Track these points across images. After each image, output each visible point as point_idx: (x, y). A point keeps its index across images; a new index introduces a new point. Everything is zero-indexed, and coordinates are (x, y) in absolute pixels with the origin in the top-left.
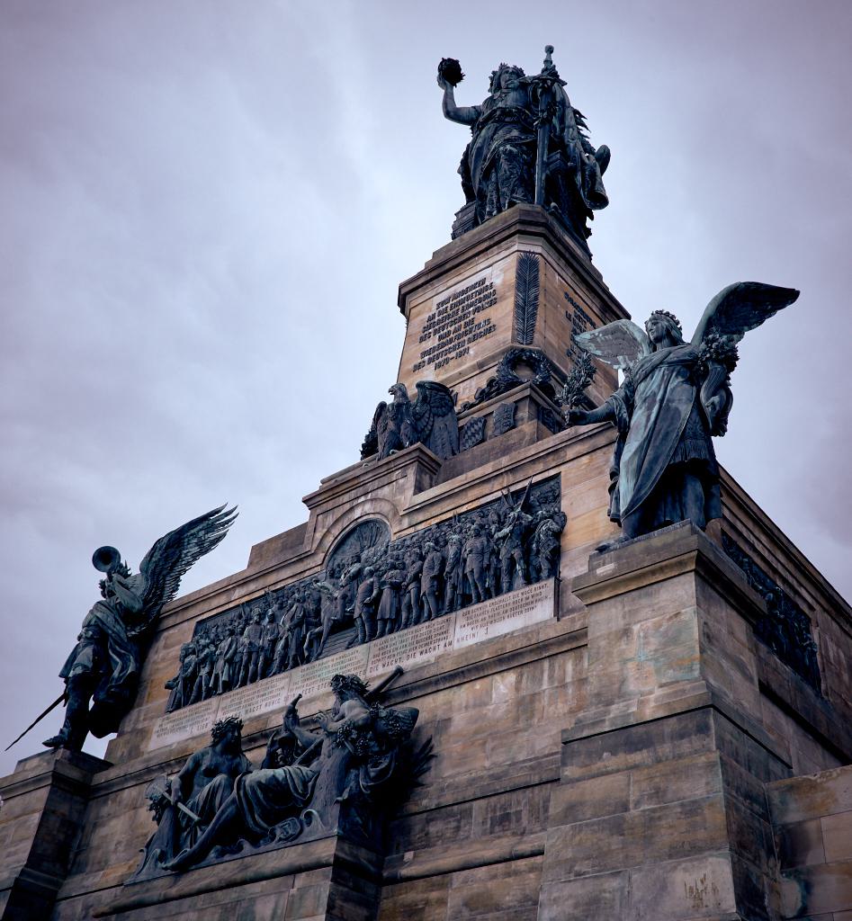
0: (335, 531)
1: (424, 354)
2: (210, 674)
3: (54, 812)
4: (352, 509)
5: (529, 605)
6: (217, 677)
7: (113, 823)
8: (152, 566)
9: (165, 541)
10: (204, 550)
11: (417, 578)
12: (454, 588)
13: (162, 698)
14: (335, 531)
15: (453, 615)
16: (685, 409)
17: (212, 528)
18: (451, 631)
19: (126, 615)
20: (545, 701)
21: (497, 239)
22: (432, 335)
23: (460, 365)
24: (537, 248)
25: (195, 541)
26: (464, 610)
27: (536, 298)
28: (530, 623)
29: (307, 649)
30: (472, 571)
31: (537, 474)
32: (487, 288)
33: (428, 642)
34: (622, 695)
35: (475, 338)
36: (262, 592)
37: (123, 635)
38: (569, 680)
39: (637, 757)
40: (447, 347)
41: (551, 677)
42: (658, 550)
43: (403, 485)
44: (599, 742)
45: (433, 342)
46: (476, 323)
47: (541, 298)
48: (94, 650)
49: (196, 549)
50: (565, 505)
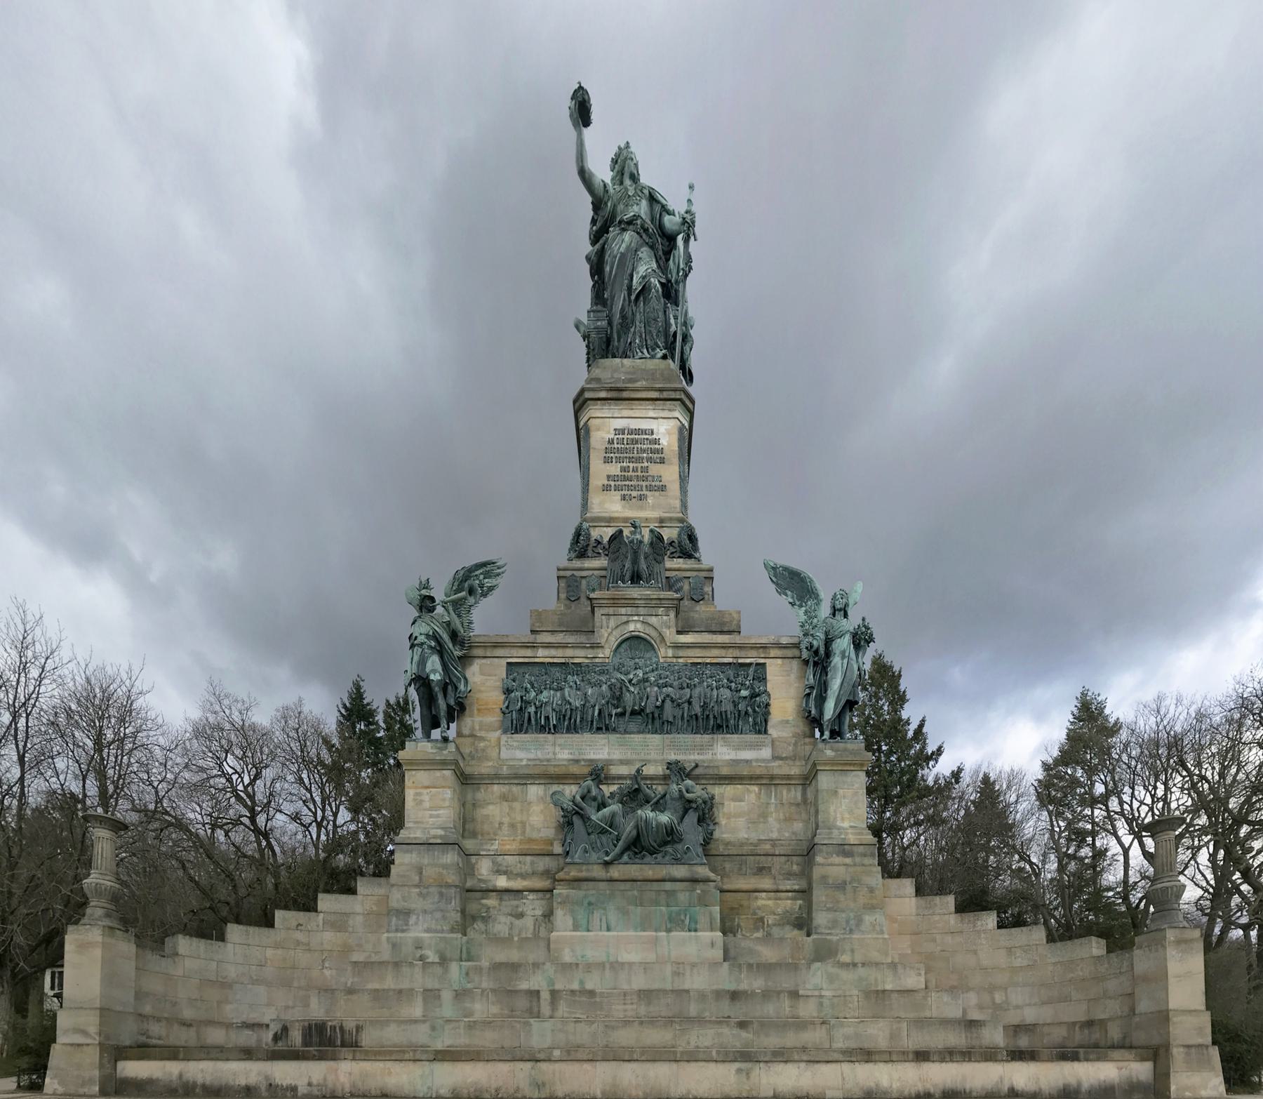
2: (536, 713)
6: (547, 718)
13: (494, 718)
39: (848, 861)
44: (831, 849)
50: (769, 688)
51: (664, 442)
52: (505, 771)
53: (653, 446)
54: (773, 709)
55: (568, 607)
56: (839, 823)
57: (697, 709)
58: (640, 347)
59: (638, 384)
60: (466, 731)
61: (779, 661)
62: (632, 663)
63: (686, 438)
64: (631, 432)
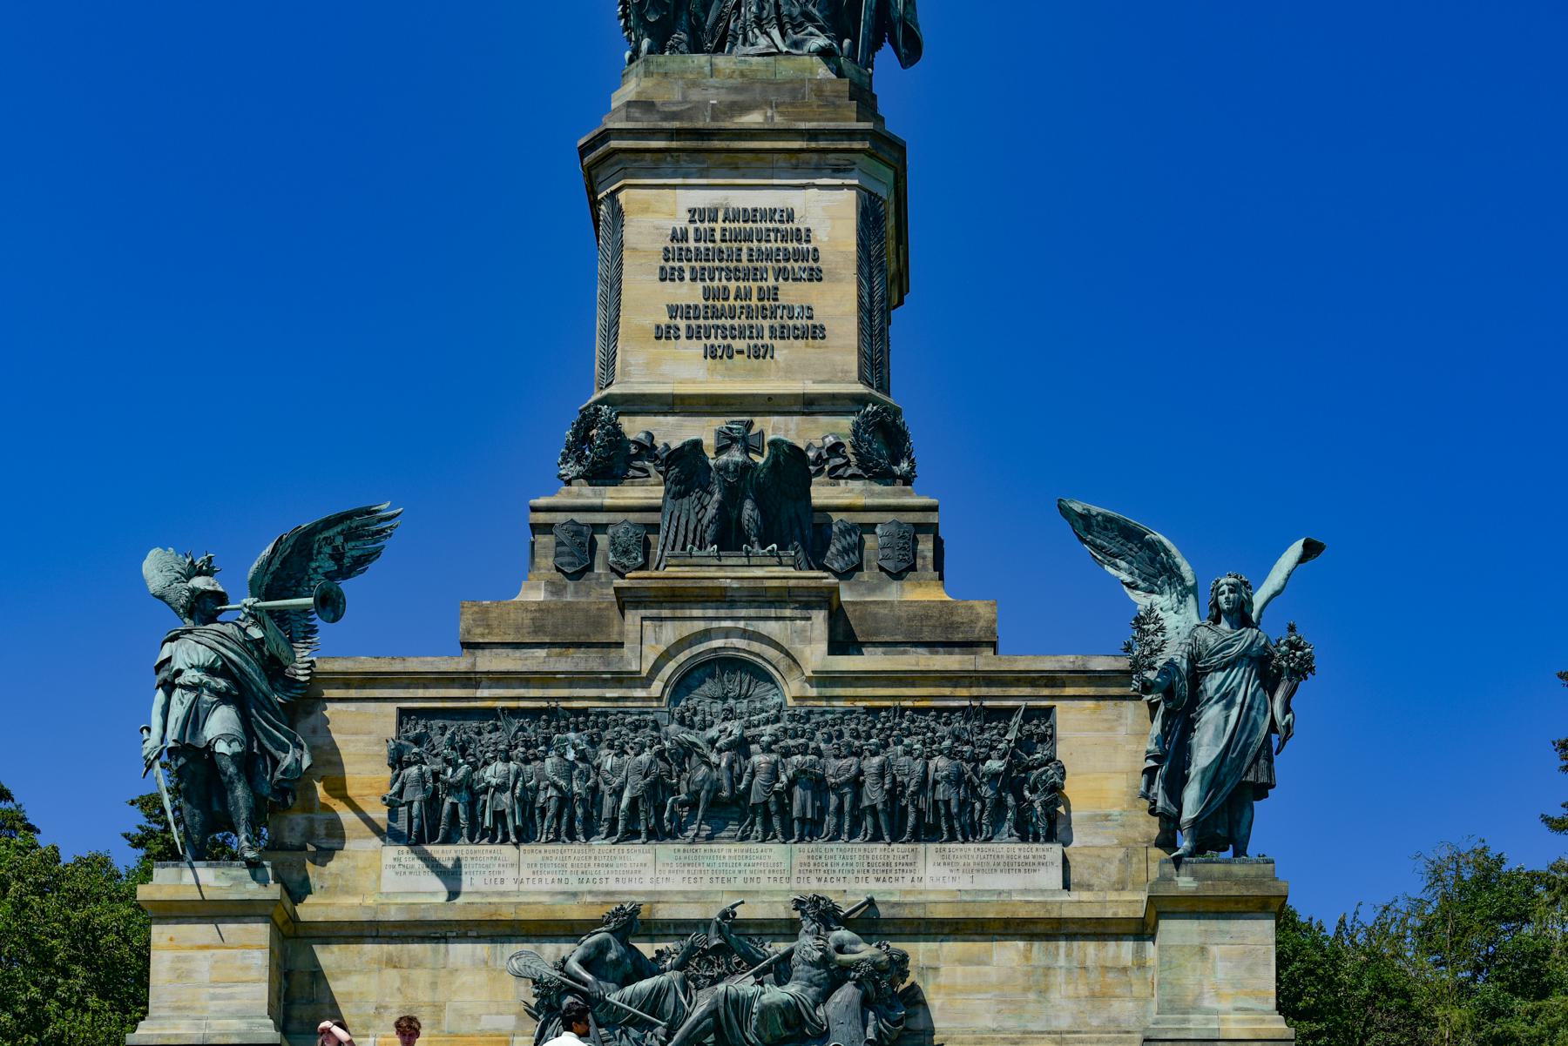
0: (682, 657)
1: (673, 311)
4: (706, 635)
5: (1029, 867)
7: (355, 979)
11: (856, 783)
12: (920, 813)
14: (682, 657)
15: (921, 847)
18: (920, 864)
20: (1059, 978)
21: (823, 144)
22: (687, 275)
23: (758, 374)
26: (938, 846)
28: (1030, 887)
29: (670, 821)
30: (947, 803)
31: (1018, 697)
32: (797, 235)
33: (886, 870)
34: (1195, 1008)
35: (782, 333)
36: (544, 704)
38: (1089, 963)
40: (719, 322)
41: (1068, 955)
42: (1238, 881)
43: (804, 630)
45: (689, 293)
46: (783, 300)
50: (1062, 753)
51: (821, 238)
52: (394, 915)
53: (790, 246)
54: (1070, 789)
55: (555, 589)
56: (1208, 1003)
57: (873, 795)
58: (759, 22)
59: (754, 119)
60: (293, 839)
61: (1090, 704)
62: (718, 707)
63: (882, 232)
64: (734, 215)
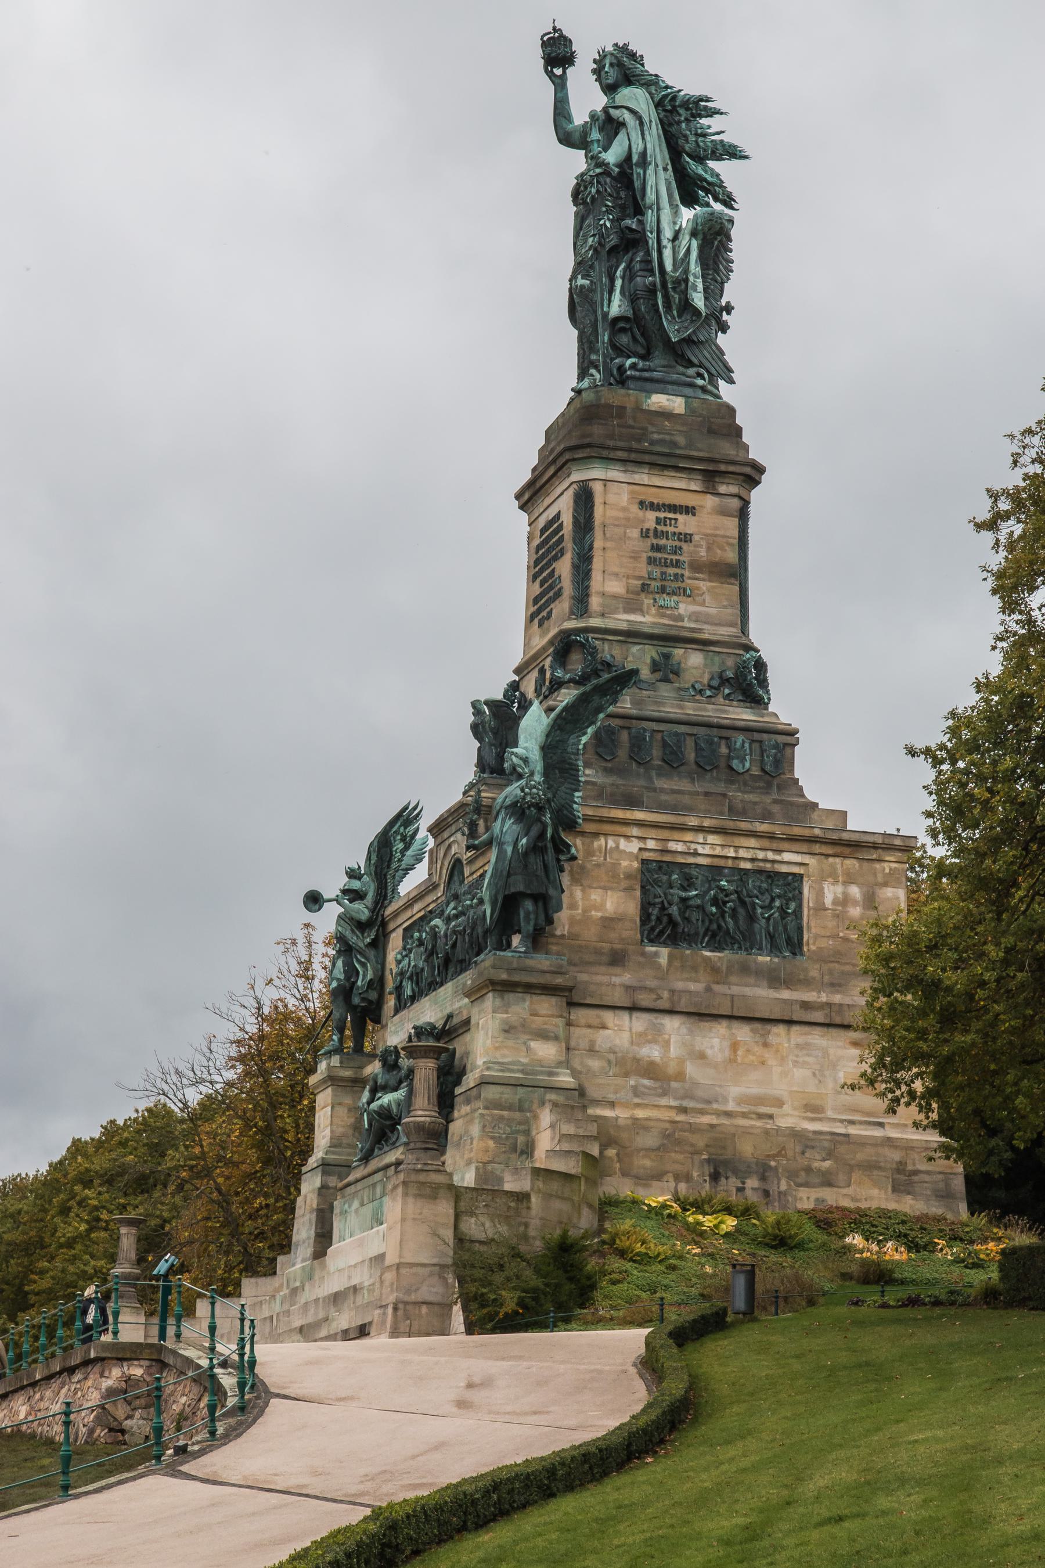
3: (340, 1104)
8: (373, 868)
9: (375, 844)
10: (407, 848)
16: (509, 850)
17: (408, 823)
19: (362, 926)
21: (559, 463)
24: (595, 472)
25: (399, 837)
27: (591, 548)
37: (361, 945)
47: (598, 544)
48: (343, 962)
49: (401, 846)
